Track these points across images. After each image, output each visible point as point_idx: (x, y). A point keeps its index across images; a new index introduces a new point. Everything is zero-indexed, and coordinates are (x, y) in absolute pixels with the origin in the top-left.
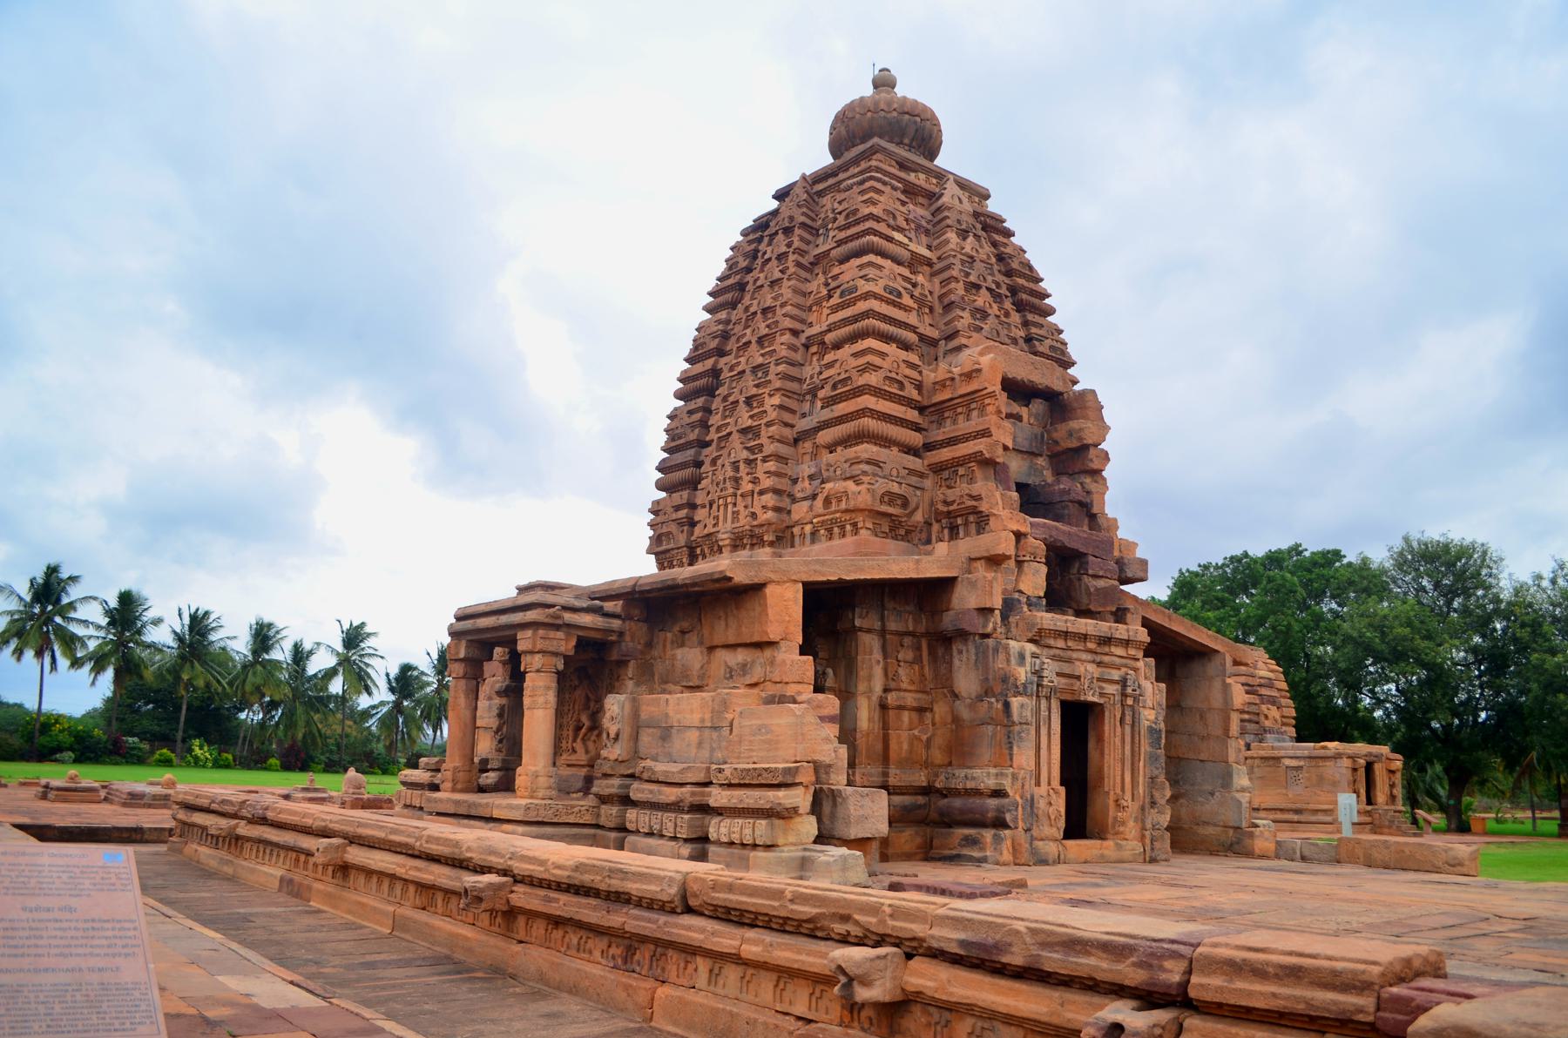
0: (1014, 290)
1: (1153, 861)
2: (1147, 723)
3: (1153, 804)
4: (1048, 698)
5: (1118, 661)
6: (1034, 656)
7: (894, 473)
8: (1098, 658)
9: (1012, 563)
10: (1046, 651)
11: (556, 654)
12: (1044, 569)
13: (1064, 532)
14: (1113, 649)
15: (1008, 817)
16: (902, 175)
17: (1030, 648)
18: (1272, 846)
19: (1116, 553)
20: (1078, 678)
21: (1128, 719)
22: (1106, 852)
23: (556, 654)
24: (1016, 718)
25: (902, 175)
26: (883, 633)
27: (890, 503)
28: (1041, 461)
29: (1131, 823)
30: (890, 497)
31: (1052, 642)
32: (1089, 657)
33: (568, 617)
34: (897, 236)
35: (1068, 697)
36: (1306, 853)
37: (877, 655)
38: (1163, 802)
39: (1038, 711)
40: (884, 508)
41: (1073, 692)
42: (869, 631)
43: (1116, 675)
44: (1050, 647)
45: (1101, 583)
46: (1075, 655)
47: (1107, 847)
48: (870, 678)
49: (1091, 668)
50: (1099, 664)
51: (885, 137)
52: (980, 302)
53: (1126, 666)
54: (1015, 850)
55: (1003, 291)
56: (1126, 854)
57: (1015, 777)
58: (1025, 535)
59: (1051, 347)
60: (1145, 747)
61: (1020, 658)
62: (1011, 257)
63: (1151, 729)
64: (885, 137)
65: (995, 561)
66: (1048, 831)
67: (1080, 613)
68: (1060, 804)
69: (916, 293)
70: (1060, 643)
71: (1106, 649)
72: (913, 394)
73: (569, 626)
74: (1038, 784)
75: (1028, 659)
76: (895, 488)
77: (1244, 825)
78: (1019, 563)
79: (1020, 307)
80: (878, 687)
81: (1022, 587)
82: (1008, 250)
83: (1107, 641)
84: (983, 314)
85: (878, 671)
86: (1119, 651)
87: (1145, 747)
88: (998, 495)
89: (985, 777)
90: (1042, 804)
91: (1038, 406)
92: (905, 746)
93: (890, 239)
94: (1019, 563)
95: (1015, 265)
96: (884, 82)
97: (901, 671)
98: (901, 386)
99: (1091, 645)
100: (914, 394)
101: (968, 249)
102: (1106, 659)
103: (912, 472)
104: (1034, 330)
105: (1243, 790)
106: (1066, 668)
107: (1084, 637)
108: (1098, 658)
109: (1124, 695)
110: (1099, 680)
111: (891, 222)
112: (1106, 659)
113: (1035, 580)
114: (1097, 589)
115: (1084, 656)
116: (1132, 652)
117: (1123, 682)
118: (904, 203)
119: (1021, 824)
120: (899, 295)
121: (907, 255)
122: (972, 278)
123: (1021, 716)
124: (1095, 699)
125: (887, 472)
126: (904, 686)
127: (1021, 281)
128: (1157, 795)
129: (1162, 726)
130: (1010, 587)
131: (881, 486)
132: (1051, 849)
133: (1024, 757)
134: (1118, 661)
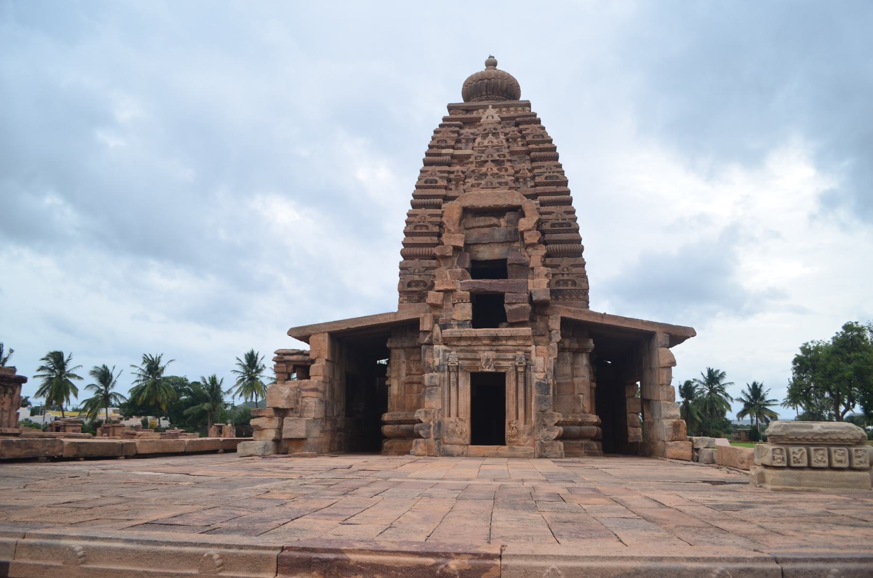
0: (528, 152)
1: (541, 457)
2: (535, 380)
3: (545, 425)
4: (458, 372)
5: (511, 348)
6: (445, 351)
7: (417, 271)
8: (495, 348)
9: (451, 306)
10: (454, 348)
11: (283, 373)
12: (469, 307)
13: (486, 284)
14: (504, 342)
15: (421, 432)
16: (468, 116)
17: (443, 347)
18: (688, 453)
19: (530, 288)
20: (480, 360)
21: (521, 379)
22: (499, 451)
23: (283, 373)
24: (426, 383)
25: (468, 116)
26: (403, 348)
27: (417, 286)
28: (516, 245)
29: (525, 437)
30: (417, 283)
31: (455, 343)
32: (487, 348)
33: (287, 358)
34: (444, 151)
35: (476, 371)
36: (715, 457)
37: (403, 359)
38: (552, 424)
39: (449, 377)
40: (410, 289)
41: (477, 368)
42: (396, 348)
43: (510, 356)
44: (455, 346)
45: (515, 306)
46: (476, 348)
47: (503, 449)
48: (399, 370)
49: (486, 354)
50: (497, 351)
51: (492, 89)
52: (484, 170)
53: (519, 350)
54: (429, 448)
55: (508, 157)
56: (518, 453)
57: (426, 413)
58: (455, 290)
59: (546, 178)
60: (535, 394)
61: (438, 354)
62: (528, 134)
63: (539, 384)
64: (492, 89)
65: (435, 306)
66: (455, 439)
67: (512, 325)
68: (466, 427)
69: (452, 176)
70: (463, 343)
71: (500, 343)
72: (436, 229)
73: (289, 361)
74: (449, 416)
75: (441, 354)
76: (417, 278)
77: (666, 439)
78: (454, 304)
79: (533, 160)
80: (403, 373)
81: (454, 317)
82: (528, 131)
83: (496, 338)
84: (485, 175)
85: (404, 367)
86: (510, 343)
87: (535, 394)
88: (447, 272)
89: (419, 415)
90: (451, 426)
91: (509, 216)
92: (415, 401)
93: (440, 155)
94: (454, 304)
95: (529, 138)
96: (491, 63)
97: (412, 365)
98: (427, 227)
99: (485, 342)
100: (436, 229)
101: (486, 143)
102: (501, 348)
103: (427, 269)
104: (536, 171)
105: (673, 417)
106: (469, 355)
107: (476, 338)
108: (495, 348)
109: (516, 367)
110: (494, 360)
111: (444, 145)
112: (501, 348)
113: (465, 311)
114: (510, 310)
115: (483, 348)
116: (521, 342)
117: (514, 359)
118: (454, 132)
119: (432, 436)
120: (436, 182)
121: (448, 158)
122: (482, 159)
123: (430, 382)
124: (490, 370)
125: (412, 270)
126: (413, 372)
127: (531, 146)
128: (547, 421)
129: (551, 381)
130: (448, 318)
131: (409, 278)
132: (458, 449)
133: (433, 403)
134: (511, 348)
